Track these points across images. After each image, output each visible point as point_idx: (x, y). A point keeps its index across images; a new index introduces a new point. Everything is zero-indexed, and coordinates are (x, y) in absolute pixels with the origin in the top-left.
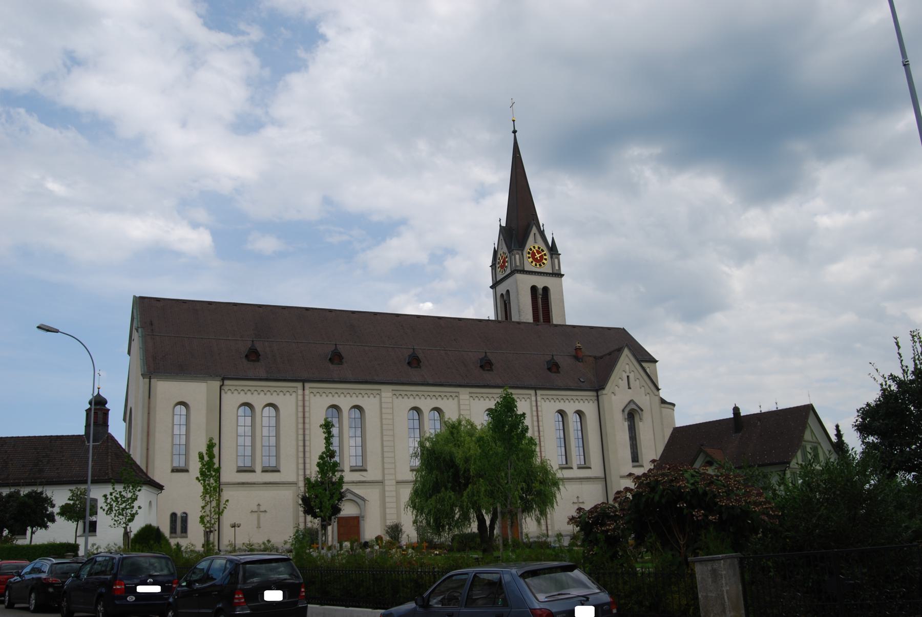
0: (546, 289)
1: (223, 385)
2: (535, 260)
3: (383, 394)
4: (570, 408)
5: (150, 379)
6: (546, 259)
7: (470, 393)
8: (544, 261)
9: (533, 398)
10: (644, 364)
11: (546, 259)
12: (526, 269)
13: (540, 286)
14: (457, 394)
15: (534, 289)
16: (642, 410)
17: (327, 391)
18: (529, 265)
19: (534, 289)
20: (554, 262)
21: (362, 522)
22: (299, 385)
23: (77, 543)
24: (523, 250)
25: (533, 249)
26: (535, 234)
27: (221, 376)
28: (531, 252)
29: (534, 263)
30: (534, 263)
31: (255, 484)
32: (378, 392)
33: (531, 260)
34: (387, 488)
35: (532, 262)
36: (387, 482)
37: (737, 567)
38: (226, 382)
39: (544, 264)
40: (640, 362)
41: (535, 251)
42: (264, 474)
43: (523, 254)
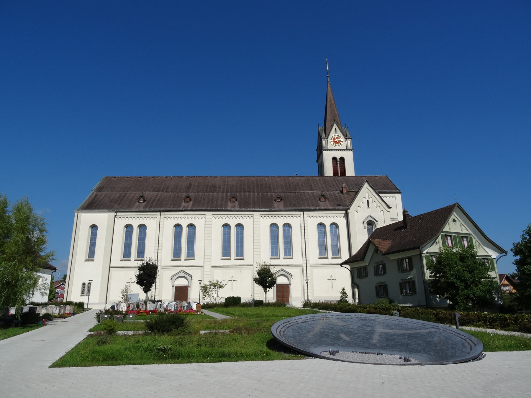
0: (342, 159)
1: (116, 216)
2: (335, 142)
3: (207, 217)
4: (327, 222)
5: (78, 213)
6: (342, 142)
7: (260, 214)
8: (341, 143)
9: (302, 216)
10: (381, 195)
11: (342, 142)
12: (329, 148)
13: (338, 157)
14: (252, 216)
15: (334, 159)
16: (377, 221)
17: (185, 216)
18: (331, 145)
19: (334, 159)
20: (348, 144)
21: (189, 289)
22: (158, 213)
23: (145, 294)
24: (327, 138)
25: (334, 137)
26: (336, 129)
27: (115, 211)
28: (333, 138)
29: (334, 145)
30: (334, 145)
31: (179, 267)
32: (204, 216)
33: (332, 143)
34: (205, 270)
35: (333, 144)
36: (205, 267)
37: (303, 350)
38: (118, 214)
39: (341, 144)
40: (377, 193)
41: (335, 138)
42: (284, 260)
43: (327, 140)
